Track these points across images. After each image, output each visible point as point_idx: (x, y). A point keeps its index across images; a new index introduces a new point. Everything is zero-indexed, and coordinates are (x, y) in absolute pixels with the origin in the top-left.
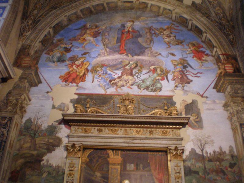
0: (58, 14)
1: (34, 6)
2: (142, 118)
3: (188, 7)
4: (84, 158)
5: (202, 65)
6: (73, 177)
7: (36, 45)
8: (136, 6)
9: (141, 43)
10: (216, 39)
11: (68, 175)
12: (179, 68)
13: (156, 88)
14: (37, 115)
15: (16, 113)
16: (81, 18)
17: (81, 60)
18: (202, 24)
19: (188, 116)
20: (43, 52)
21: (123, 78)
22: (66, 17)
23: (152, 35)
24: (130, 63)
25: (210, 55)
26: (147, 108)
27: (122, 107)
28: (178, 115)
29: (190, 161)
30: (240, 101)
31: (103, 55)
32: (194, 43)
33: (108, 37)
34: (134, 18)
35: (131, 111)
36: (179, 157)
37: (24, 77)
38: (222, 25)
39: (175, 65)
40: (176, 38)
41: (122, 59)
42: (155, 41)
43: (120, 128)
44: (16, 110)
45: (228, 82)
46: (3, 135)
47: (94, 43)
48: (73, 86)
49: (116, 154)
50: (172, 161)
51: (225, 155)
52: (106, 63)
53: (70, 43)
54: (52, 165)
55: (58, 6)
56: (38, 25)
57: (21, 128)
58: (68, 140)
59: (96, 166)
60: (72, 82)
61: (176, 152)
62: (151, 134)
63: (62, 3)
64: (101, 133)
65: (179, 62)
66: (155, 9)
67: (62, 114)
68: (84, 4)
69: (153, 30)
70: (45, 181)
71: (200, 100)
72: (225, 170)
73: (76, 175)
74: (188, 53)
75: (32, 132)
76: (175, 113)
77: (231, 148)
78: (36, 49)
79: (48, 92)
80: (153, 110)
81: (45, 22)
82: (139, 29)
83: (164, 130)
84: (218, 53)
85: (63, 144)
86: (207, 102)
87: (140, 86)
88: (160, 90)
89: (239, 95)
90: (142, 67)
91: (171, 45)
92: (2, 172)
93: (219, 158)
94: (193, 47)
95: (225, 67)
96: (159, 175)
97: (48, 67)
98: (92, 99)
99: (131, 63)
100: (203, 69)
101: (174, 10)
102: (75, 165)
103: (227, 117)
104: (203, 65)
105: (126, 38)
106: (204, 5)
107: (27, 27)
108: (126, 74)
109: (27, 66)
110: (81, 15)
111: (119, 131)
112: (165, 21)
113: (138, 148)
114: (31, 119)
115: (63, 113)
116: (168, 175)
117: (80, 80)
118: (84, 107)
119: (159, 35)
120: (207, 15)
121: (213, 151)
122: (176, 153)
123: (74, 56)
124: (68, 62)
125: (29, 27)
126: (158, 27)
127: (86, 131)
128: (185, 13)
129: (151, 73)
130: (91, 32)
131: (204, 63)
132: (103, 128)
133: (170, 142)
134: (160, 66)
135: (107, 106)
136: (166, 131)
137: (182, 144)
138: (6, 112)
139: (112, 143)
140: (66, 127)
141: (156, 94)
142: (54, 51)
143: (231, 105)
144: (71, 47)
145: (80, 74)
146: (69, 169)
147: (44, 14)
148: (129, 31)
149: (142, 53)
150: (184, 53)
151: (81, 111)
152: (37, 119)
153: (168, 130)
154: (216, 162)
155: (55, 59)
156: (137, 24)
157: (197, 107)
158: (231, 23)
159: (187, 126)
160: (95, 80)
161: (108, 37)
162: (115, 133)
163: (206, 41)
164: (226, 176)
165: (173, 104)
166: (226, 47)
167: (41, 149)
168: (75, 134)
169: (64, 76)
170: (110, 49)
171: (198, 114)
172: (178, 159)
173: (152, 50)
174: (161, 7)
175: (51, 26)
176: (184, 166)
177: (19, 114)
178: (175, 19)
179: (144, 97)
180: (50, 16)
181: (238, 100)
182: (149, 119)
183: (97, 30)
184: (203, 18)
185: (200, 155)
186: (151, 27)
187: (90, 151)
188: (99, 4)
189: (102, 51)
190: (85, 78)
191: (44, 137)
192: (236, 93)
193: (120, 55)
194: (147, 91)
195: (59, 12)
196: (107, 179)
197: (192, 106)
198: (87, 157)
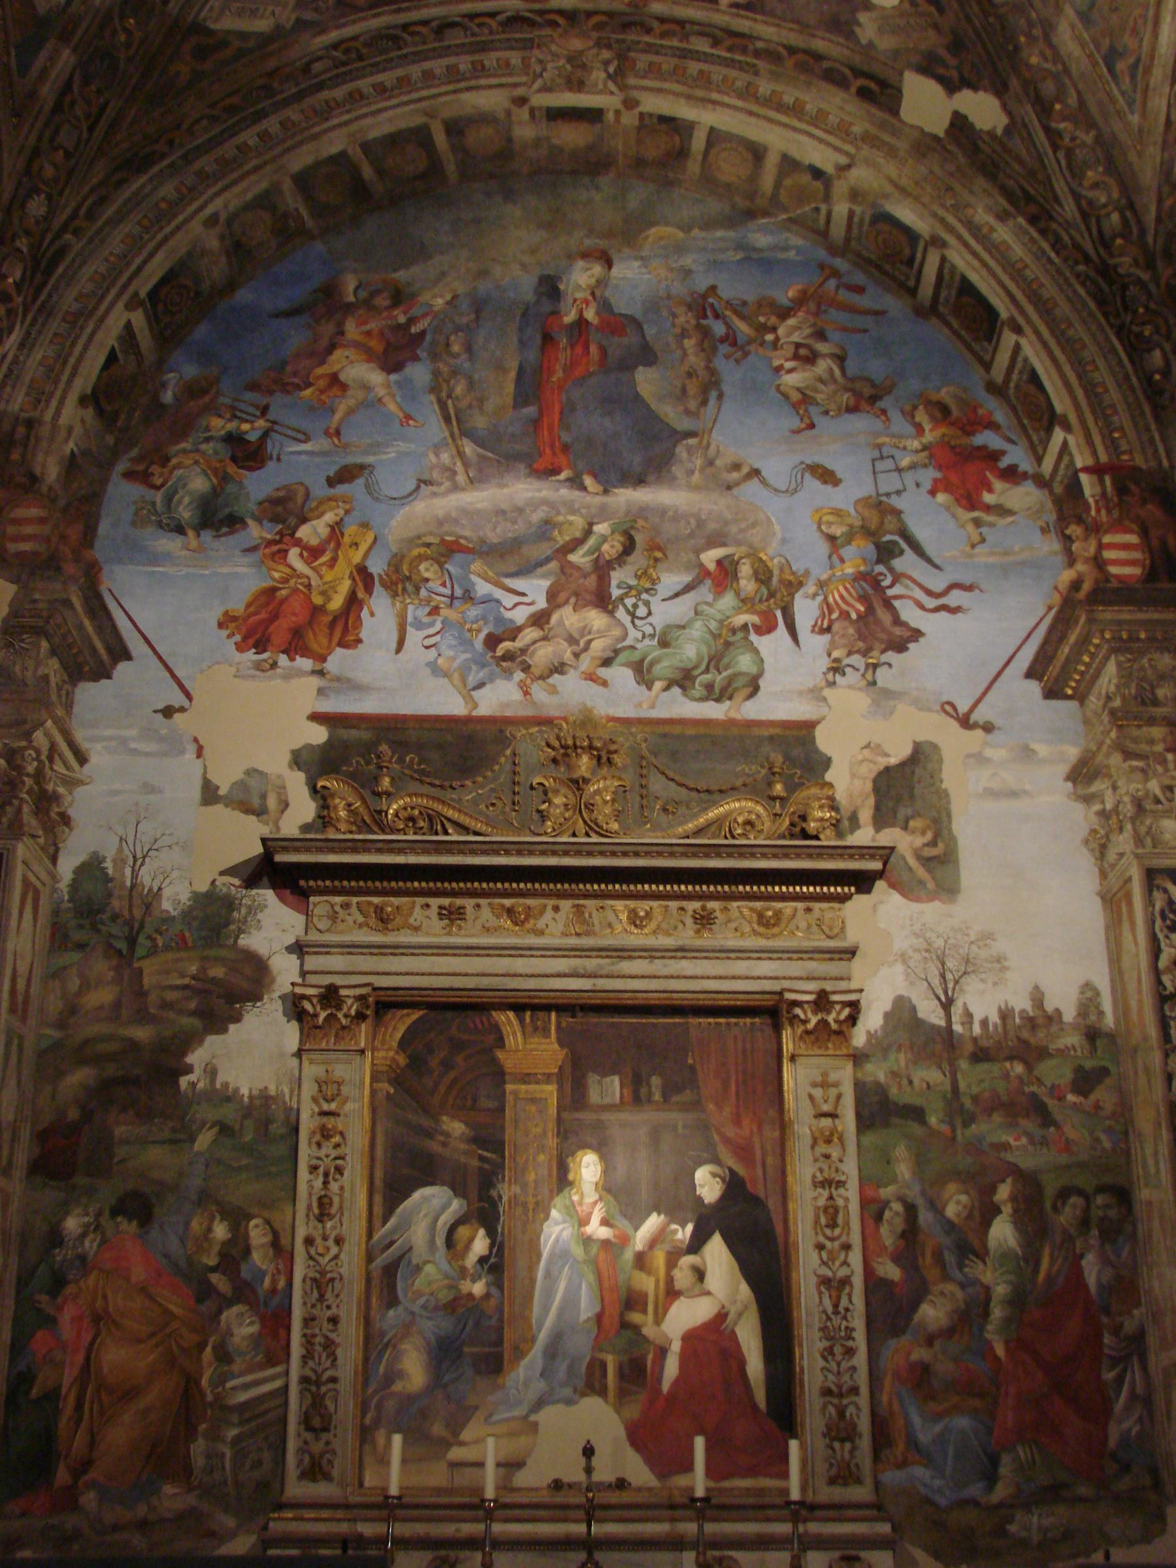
0: (163, 205)
1: (28, 172)
2: (660, 854)
3: (925, 145)
4: (381, 1054)
5: (976, 538)
6: (337, 1146)
7: (63, 421)
11: (318, 1137)
12: (856, 556)
13: (731, 680)
14: (131, 840)
17: (329, 517)
18: (999, 271)
20: (111, 465)
21: (561, 623)
23: (714, 350)
24: (596, 528)
25: (1025, 476)
26: (684, 791)
27: (556, 792)
28: (836, 824)
29: (885, 1058)
30: (1159, 748)
31: (447, 484)
32: (948, 400)
34: (610, 234)
35: (604, 814)
36: (833, 1037)
37: (32, 621)
39: (832, 539)
40: (849, 364)
41: (551, 505)
42: (725, 388)
43: (551, 902)
44: (19, 811)
45: (1107, 636)
47: (392, 407)
48: (300, 673)
49: (536, 1029)
50: (800, 1060)
52: (467, 533)
53: (257, 407)
54: (237, 1090)
56: (56, 288)
57: (56, 912)
58: (302, 965)
59: (442, 1088)
61: (819, 1017)
62: (703, 925)
63: (185, 126)
64: (460, 927)
65: (858, 523)
66: (730, 169)
67: (264, 841)
68: (317, 129)
69: (717, 316)
70: (207, 1166)
72: (1051, 1103)
73: (349, 1136)
74: (905, 462)
76: (822, 820)
77: (1089, 994)
78: (71, 445)
79: (168, 712)
80: (715, 804)
81: (95, 267)
82: (636, 311)
83: (767, 904)
84: (1072, 462)
85: (275, 986)
86: (989, 753)
87: (649, 670)
88: (754, 687)
89: (1160, 711)
90: (658, 554)
91: (813, 410)
93: (1025, 1043)
95: (1101, 547)
96: (737, 1121)
97: (155, 559)
98: (401, 747)
99: (601, 528)
100: (983, 560)
101: (843, 169)
102: (345, 1090)
103: (1084, 833)
104: (983, 540)
108: (573, 600)
109: (36, 554)
110: (304, 213)
111: (549, 913)
112: (785, 249)
113: (641, 999)
114: (104, 859)
115: (266, 831)
116: (783, 1126)
117: (331, 635)
118: (367, 794)
119: (752, 348)
120: (1033, 209)
122: (823, 1023)
123: (285, 487)
124: (256, 532)
125: (10, 306)
126: (745, 297)
127: (383, 920)
129: (705, 592)
130: (368, 333)
131: (992, 525)
132: (468, 903)
133: (795, 968)
134: (751, 546)
135: (482, 787)
136: (778, 914)
137: (849, 979)
139: (515, 975)
140: (282, 899)
142: (174, 461)
143: (1108, 767)
144: (266, 435)
145: (329, 599)
146: (316, 1110)
147: (82, 212)
148: (581, 322)
150: (888, 464)
152: (131, 861)
153: (787, 907)
154: (1008, 1064)
155: (185, 513)
156: (630, 275)
157: (934, 777)
159: (880, 885)
160: (414, 637)
161: (467, 365)
162: (529, 925)
163: (1012, 385)
164: (1052, 1129)
166: (1123, 418)
167: (172, 1015)
169: (245, 619)
170: (482, 446)
172: (830, 1052)
173: (713, 447)
174: (766, 149)
175: (136, 294)
177: (34, 836)
178: (847, 240)
179: (667, 729)
180: (120, 217)
181: (1151, 742)
182: (695, 855)
183: (402, 319)
184: (1011, 223)
185: (934, 1027)
186: (704, 297)
187: (408, 1015)
188: (400, 132)
189: (437, 455)
191: (183, 954)
192: (1146, 698)
194: (686, 695)
195: (168, 190)
196: (499, 1147)
197: (913, 773)
198: (395, 1044)
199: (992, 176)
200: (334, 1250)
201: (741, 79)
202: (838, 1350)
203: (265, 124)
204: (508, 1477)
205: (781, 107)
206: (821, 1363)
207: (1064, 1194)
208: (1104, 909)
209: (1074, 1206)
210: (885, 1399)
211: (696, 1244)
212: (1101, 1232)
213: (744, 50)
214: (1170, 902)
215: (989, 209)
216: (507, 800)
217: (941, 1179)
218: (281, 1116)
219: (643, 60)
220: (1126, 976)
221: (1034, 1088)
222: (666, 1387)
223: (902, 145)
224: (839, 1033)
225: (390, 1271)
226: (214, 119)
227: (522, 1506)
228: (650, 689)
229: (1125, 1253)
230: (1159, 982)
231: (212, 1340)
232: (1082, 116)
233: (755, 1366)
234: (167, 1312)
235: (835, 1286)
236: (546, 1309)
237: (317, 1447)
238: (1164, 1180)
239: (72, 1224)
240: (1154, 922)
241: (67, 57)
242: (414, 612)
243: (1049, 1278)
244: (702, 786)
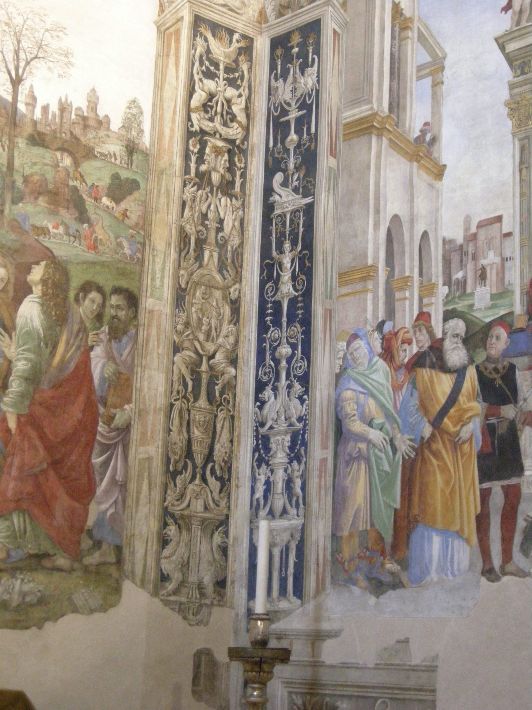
51: (102, 133)
72: (89, 202)
77: (134, 111)
121: (60, 99)
154: (58, 154)
164: (86, 225)
208: (158, 40)
209: (93, 301)
212: (110, 328)
214: (208, 51)
220: (165, 105)
221: (77, 183)
229: (126, 353)
230: (189, 119)
238: (165, 295)
240: (193, 64)
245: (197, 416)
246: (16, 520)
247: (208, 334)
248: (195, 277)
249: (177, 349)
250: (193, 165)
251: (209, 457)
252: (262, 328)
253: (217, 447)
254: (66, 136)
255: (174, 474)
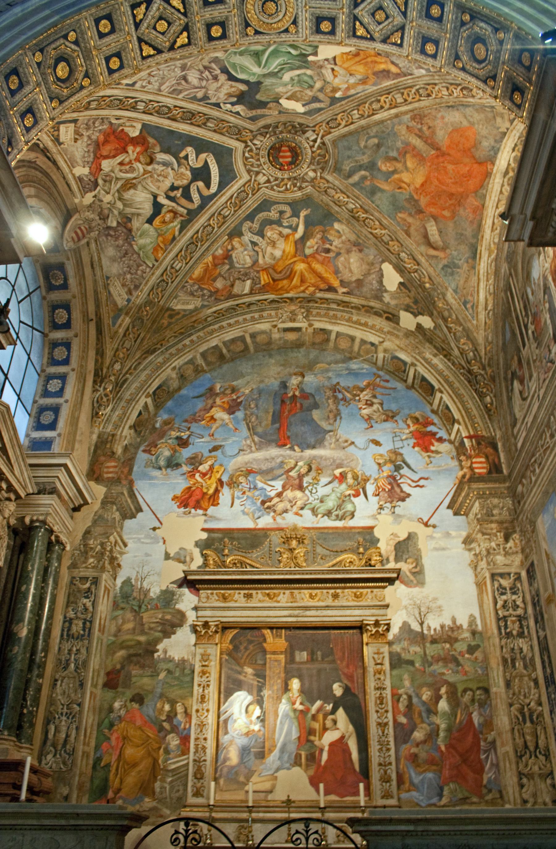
1: (115, 356)
3: (408, 334)
7: (124, 434)
8: (307, 338)
9: (319, 422)
10: (459, 404)
12: (388, 469)
13: (345, 513)
15: (103, 569)
16: (204, 371)
19: (399, 565)
20: (137, 448)
22: (175, 372)
23: (339, 403)
25: (445, 440)
29: (400, 643)
30: (494, 531)
32: (418, 416)
33: (255, 410)
35: (301, 560)
38: (471, 375)
39: (379, 464)
42: (343, 415)
43: (282, 591)
46: (86, 609)
47: (231, 426)
48: (199, 515)
55: (159, 346)
57: (115, 597)
60: (195, 508)
66: (344, 344)
67: (184, 572)
71: (421, 531)
72: (460, 658)
74: (404, 437)
75: (134, 603)
78: (126, 442)
79: (154, 529)
80: (339, 556)
81: (136, 385)
86: (435, 535)
88: (352, 515)
89: (494, 518)
92: (91, 674)
93: (449, 637)
94: (414, 424)
95: (472, 463)
97: (151, 478)
98: (232, 539)
99: (300, 464)
102: (211, 657)
103: (469, 562)
105: (290, 411)
106: (438, 332)
107: (105, 399)
111: (282, 595)
112: (362, 369)
113: (313, 625)
115: (186, 568)
116: (364, 668)
118: (220, 555)
120: (445, 352)
122: (377, 631)
124: (185, 468)
127: (225, 598)
128: (401, 349)
129: (336, 483)
132: (254, 592)
136: (361, 593)
138: (86, 567)
140: (191, 592)
141: (346, 525)
144: (189, 436)
148: (294, 396)
149: (319, 443)
150: (398, 438)
151: (217, 565)
153: (365, 591)
155: (162, 463)
157: (416, 544)
158: (489, 371)
159: (397, 582)
160: (237, 502)
165: (374, 541)
166: (478, 420)
167: (152, 632)
168: (207, 605)
171: (418, 561)
176: (390, 653)
178: (383, 365)
180: (145, 369)
181: (492, 529)
183: (235, 397)
185: (417, 632)
190: (218, 497)
192: (489, 514)
193: (279, 450)
195: (160, 359)
196: (264, 677)
199: (431, 343)
200: (206, 714)
201: (347, 316)
202: (384, 749)
203: (192, 337)
204: (266, 796)
205: (360, 324)
206: (378, 754)
207: (465, 691)
210: (401, 767)
211: (334, 711)
213: (348, 307)
214: (500, 585)
215: (430, 353)
216: (267, 555)
217: (420, 686)
218: (188, 667)
219: (315, 312)
221: (453, 653)
222: (323, 763)
223: (401, 334)
224: (383, 635)
225: (226, 721)
226: (176, 337)
227: (273, 807)
228: (317, 516)
231: (163, 746)
232: (458, 322)
233: (355, 755)
234: (148, 736)
235: (382, 725)
236: (280, 735)
237: (199, 785)
239: (117, 705)
241: (128, 320)
242: (237, 493)
243: (461, 722)
244: (334, 549)
245: (527, 730)
246: (452, 785)
247: (525, 696)
248: (514, 674)
249: (511, 705)
250: (503, 631)
251: (537, 746)
252: (547, 689)
253: (540, 742)
254: (445, 637)
255: (521, 757)
